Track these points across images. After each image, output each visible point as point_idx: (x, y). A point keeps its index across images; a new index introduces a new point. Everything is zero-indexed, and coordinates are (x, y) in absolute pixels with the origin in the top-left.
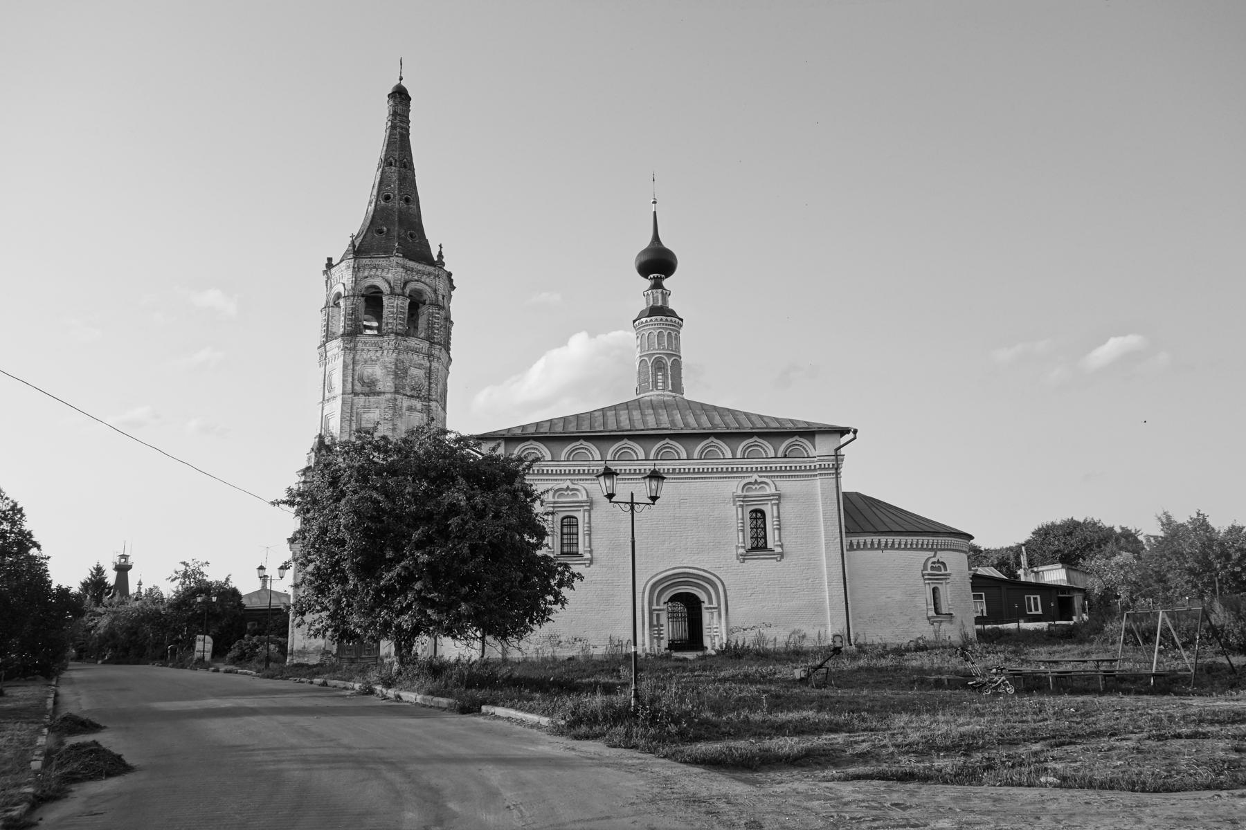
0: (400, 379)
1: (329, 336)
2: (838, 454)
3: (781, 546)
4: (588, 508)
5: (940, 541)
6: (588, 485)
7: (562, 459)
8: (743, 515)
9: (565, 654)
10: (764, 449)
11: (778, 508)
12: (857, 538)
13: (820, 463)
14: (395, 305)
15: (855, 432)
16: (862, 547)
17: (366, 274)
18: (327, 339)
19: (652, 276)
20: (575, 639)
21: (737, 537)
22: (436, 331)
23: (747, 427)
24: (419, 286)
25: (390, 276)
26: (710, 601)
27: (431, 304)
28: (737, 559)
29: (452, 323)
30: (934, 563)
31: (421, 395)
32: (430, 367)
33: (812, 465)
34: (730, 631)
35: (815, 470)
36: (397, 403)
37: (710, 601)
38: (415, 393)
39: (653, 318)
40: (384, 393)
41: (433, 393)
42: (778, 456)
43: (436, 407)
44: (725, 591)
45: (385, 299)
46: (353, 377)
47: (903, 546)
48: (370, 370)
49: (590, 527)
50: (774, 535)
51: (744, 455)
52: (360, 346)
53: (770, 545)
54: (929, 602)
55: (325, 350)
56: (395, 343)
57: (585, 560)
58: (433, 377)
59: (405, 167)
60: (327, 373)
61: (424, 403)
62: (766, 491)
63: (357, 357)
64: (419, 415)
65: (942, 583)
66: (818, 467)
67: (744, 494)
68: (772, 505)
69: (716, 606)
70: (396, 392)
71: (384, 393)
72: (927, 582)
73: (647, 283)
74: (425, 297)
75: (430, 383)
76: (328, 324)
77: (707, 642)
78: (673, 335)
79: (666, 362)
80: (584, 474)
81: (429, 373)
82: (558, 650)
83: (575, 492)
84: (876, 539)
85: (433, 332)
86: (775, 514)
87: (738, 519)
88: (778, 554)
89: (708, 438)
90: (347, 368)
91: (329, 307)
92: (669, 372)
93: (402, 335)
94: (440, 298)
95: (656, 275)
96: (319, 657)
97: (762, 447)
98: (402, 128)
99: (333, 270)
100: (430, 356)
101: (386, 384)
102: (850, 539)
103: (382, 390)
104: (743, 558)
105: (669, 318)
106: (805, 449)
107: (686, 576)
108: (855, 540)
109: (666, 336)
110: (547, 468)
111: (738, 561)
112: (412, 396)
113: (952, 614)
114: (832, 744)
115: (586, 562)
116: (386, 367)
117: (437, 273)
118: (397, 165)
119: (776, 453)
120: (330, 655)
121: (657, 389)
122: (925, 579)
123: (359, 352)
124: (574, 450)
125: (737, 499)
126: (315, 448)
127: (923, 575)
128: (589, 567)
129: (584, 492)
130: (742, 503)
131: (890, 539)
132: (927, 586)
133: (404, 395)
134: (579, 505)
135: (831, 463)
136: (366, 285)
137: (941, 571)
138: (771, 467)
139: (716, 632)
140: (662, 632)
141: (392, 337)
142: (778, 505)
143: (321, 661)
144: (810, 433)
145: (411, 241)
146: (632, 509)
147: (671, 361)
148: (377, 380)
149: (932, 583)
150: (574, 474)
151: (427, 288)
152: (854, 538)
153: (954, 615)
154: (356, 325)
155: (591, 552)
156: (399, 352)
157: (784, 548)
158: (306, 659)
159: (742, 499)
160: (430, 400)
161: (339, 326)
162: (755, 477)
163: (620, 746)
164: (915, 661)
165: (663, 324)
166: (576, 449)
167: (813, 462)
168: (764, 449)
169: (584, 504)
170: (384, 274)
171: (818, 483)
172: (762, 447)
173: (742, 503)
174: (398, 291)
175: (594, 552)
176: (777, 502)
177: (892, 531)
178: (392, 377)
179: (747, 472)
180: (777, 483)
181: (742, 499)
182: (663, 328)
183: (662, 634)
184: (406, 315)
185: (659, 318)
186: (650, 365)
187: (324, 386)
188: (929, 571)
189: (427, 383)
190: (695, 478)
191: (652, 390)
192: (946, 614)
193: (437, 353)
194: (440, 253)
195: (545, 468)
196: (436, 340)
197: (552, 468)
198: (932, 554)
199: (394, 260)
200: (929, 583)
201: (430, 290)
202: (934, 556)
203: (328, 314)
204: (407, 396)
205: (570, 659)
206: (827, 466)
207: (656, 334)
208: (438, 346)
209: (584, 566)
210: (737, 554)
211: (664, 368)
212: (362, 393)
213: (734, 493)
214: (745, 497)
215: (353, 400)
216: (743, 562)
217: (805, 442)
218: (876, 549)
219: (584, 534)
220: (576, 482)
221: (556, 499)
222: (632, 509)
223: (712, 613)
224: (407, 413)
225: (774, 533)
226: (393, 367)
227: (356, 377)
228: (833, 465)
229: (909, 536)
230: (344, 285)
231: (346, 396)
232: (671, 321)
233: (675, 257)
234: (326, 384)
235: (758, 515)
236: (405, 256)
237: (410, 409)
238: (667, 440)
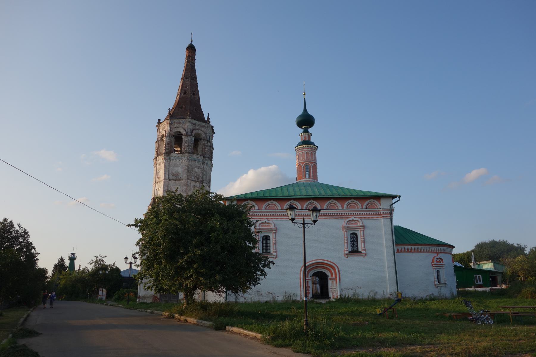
0: (190, 173)
1: (158, 154)
2: (392, 207)
3: (365, 250)
4: (275, 232)
5: (438, 249)
6: (275, 221)
7: (263, 209)
8: (347, 235)
9: (264, 300)
10: (356, 205)
11: (363, 232)
12: (401, 247)
13: (383, 211)
14: (188, 140)
15: (400, 197)
16: (403, 251)
17: (175, 126)
18: (157, 155)
19: (303, 127)
20: (269, 293)
21: (345, 246)
22: (206, 152)
23: (348, 195)
24: (199, 131)
25: (186, 127)
26: (332, 276)
27: (204, 140)
28: (345, 256)
29: (213, 148)
30: (437, 259)
31: (199, 181)
32: (203, 168)
33: (379, 212)
34: (341, 290)
35: (381, 215)
36: (188, 184)
37: (332, 276)
39: (304, 146)
40: (182, 179)
41: (204, 179)
42: (364, 208)
44: (339, 271)
45: (183, 137)
46: (169, 172)
47: (422, 251)
48: (176, 169)
49: (276, 240)
50: (362, 245)
51: (347, 207)
52: (172, 158)
53: (360, 250)
54: (435, 277)
55: (157, 160)
56: (188, 157)
57: (274, 255)
58: (205, 173)
59: (193, 79)
60: (157, 171)
61: (200, 184)
62: (358, 224)
63: (171, 163)
65: (441, 268)
66: (382, 213)
67: (347, 226)
68: (361, 231)
69: (335, 278)
70: (188, 179)
71: (182, 179)
72: (434, 268)
73: (301, 130)
74: (201, 137)
75: (203, 175)
76: (158, 149)
77: (331, 295)
78: (313, 153)
79: (310, 166)
80: (273, 216)
82: (261, 298)
83: (269, 224)
84: (410, 247)
85: (205, 152)
86: (362, 235)
87: (344, 238)
88: (364, 254)
89: (330, 200)
90: (166, 168)
91: (158, 141)
92: (312, 170)
93: (191, 154)
94: (208, 137)
95: (305, 127)
96: (151, 300)
97: (355, 204)
98: (192, 62)
99: (161, 125)
100: (203, 163)
101: (183, 175)
102: (397, 247)
103: (182, 178)
104: (347, 255)
105: (311, 146)
106: (376, 205)
107: (320, 264)
108: (400, 248)
109: (310, 154)
110: (256, 213)
111: (345, 257)
112: (195, 181)
113: (446, 283)
114: (414, 352)
115: (274, 257)
116: (183, 168)
117: (207, 126)
118: (190, 78)
119: (362, 206)
120: (157, 299)
121: (306, 178)
122: (433, 267)
123: (171, 161)
124: (268, 205)
125: (344, 228)
126: (151, 204)
127: (432, 265)
128: (275, 259)
129: (273, 224)
130: (346, 230)
131: (416, 247)
132: (434, 270)
133: (192, 180)
134: (271, 230)
135: (388, 212)
136: (175, 131)
137: (440, 263)
138: (360, 213)
139: (335, 290)
140: (309, 290)
141: (187, 154)
142: (363, 231)
143: (152, 301)
144: (378, 197)
145: (195, 112)
146: (304, 226)
147: (313, 165)
148: (179, 173)
149: (437, 268)
150: (269, 216)
151: (202, 132)
152: (402, 247)
153: (447, 283)
154: (170, 149)
155: (276, 252)
156: (189, 161)
157: (367, 251)
158: (146, 300)
159: (346, 228)
160: (203, 183)
161: (163, 150)
162: (352, 218)
163: (300, 352)
164: (434, 306)
165: (309, 148)
166: (269, 205)
167: (380, 211)
168: (356, 205)
169: (273, 230)
170: (183, 126)
171: (382, 220)
172: (355, 204)
173: (346, 230)
174: (189, 133)
175: (278, 252)
176: (363, 229)
177: (417, 244)
178: (186, 172)
179: (348, 215)
180: (363, 221)
181: (346, 228)
182: (309, 150)
183: (309, 291)
184: (193, 144)
185: (307, 146)
186: (303, 167)
187: (156, 176)
188: (435, 263)
189: (202, 175)
190: (324, 218)
191: (304, 178)
192: (443, 283)
193: (206, 161)
194: (208, 117)
195: (255, 213)
196: (206, 156)
197: (258, 213)
198: (436, 254)
199: (188, 120)
200: (435, 269)
201: (203, 133)
202: (437, 256)
203: (158, 144)
205: (267, 302)
206: (386, 213)
207: (305, 153)
208: (207, 159)
209: (273, 259)
210: (344, 254)
211: (309, 168)
212: (173, 180)
213: (342, 225)
214: (348, 227)
215: (168, 182)
216: (347, 257)
217: (376, 202)
218: (410, 252)
219: (273, 244)
220: (269, 220)
221: (260, 228)
222: (304, 226)
223: (333, 281)
225: (362, 244)
226: (187, 167)
227: (170, 172)
228: (389, 212)
229: (425, 246)
230: (165, 131)
231: (166, 181)
232: (312, 147)
233: (314, 118)
234: (157, 176)
235: (354, 236)
236: (193, 118)
238: (311, 201)
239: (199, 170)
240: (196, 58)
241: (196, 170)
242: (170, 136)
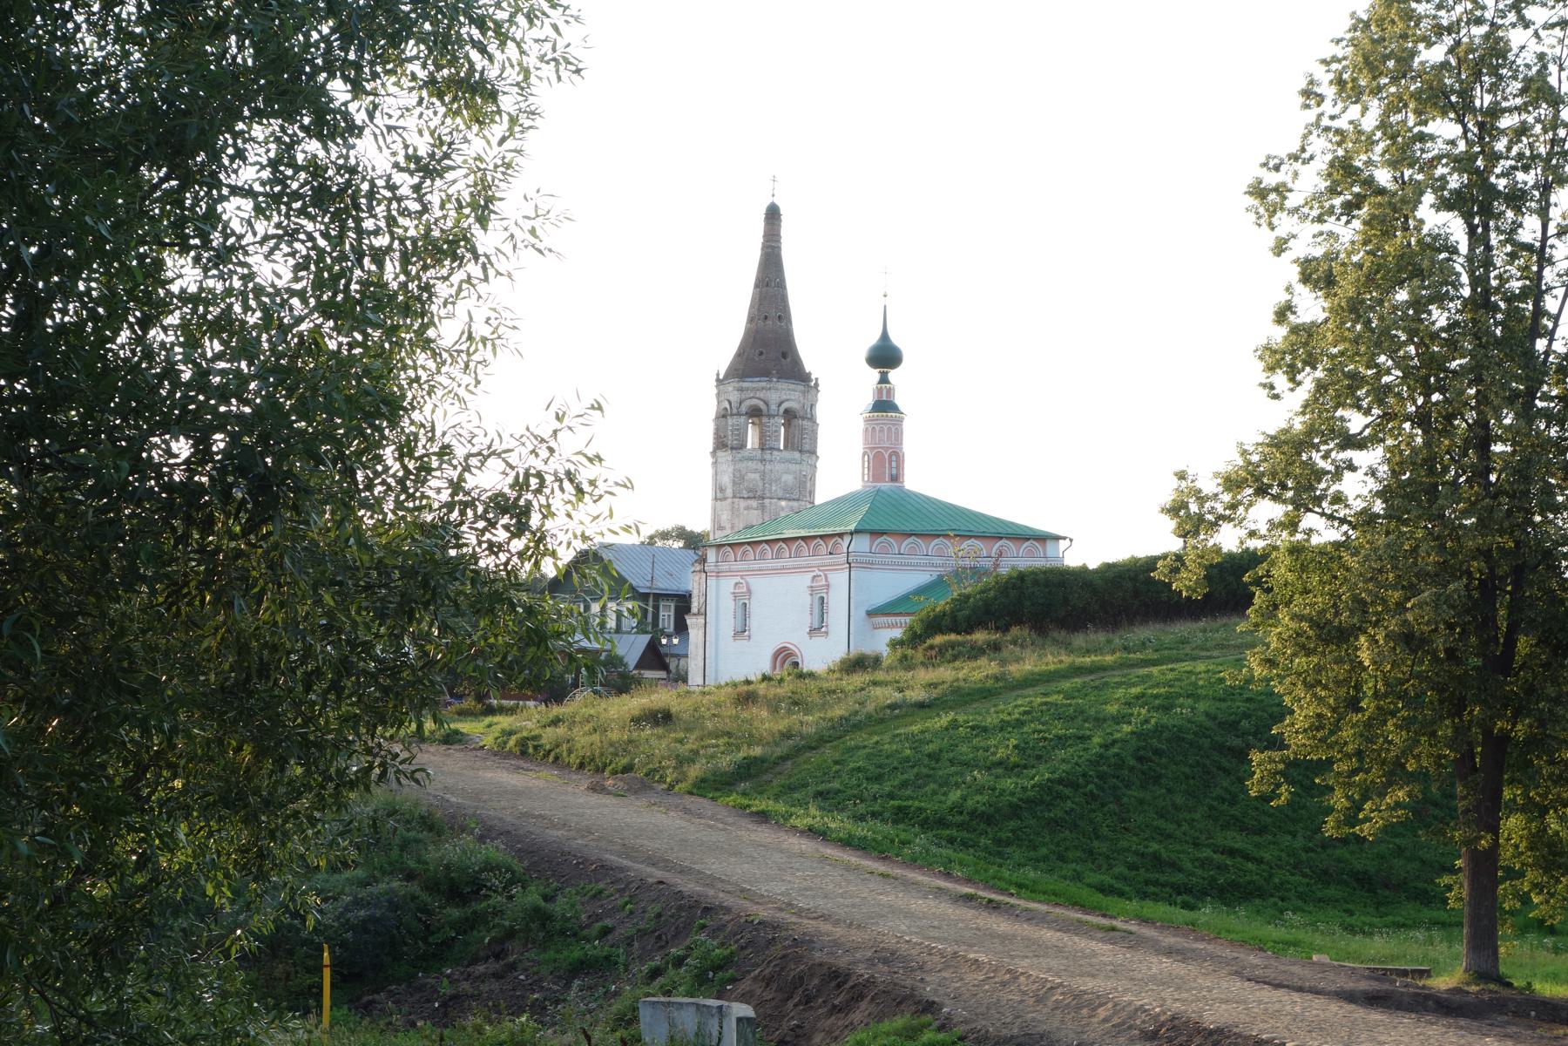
24: (755, 402)
38: (751, 495)
70: (734, 497)
100: (763, 460)
101: (729, 492)
237: (747, 508)
239: (757, 476)
241: (752, 476)
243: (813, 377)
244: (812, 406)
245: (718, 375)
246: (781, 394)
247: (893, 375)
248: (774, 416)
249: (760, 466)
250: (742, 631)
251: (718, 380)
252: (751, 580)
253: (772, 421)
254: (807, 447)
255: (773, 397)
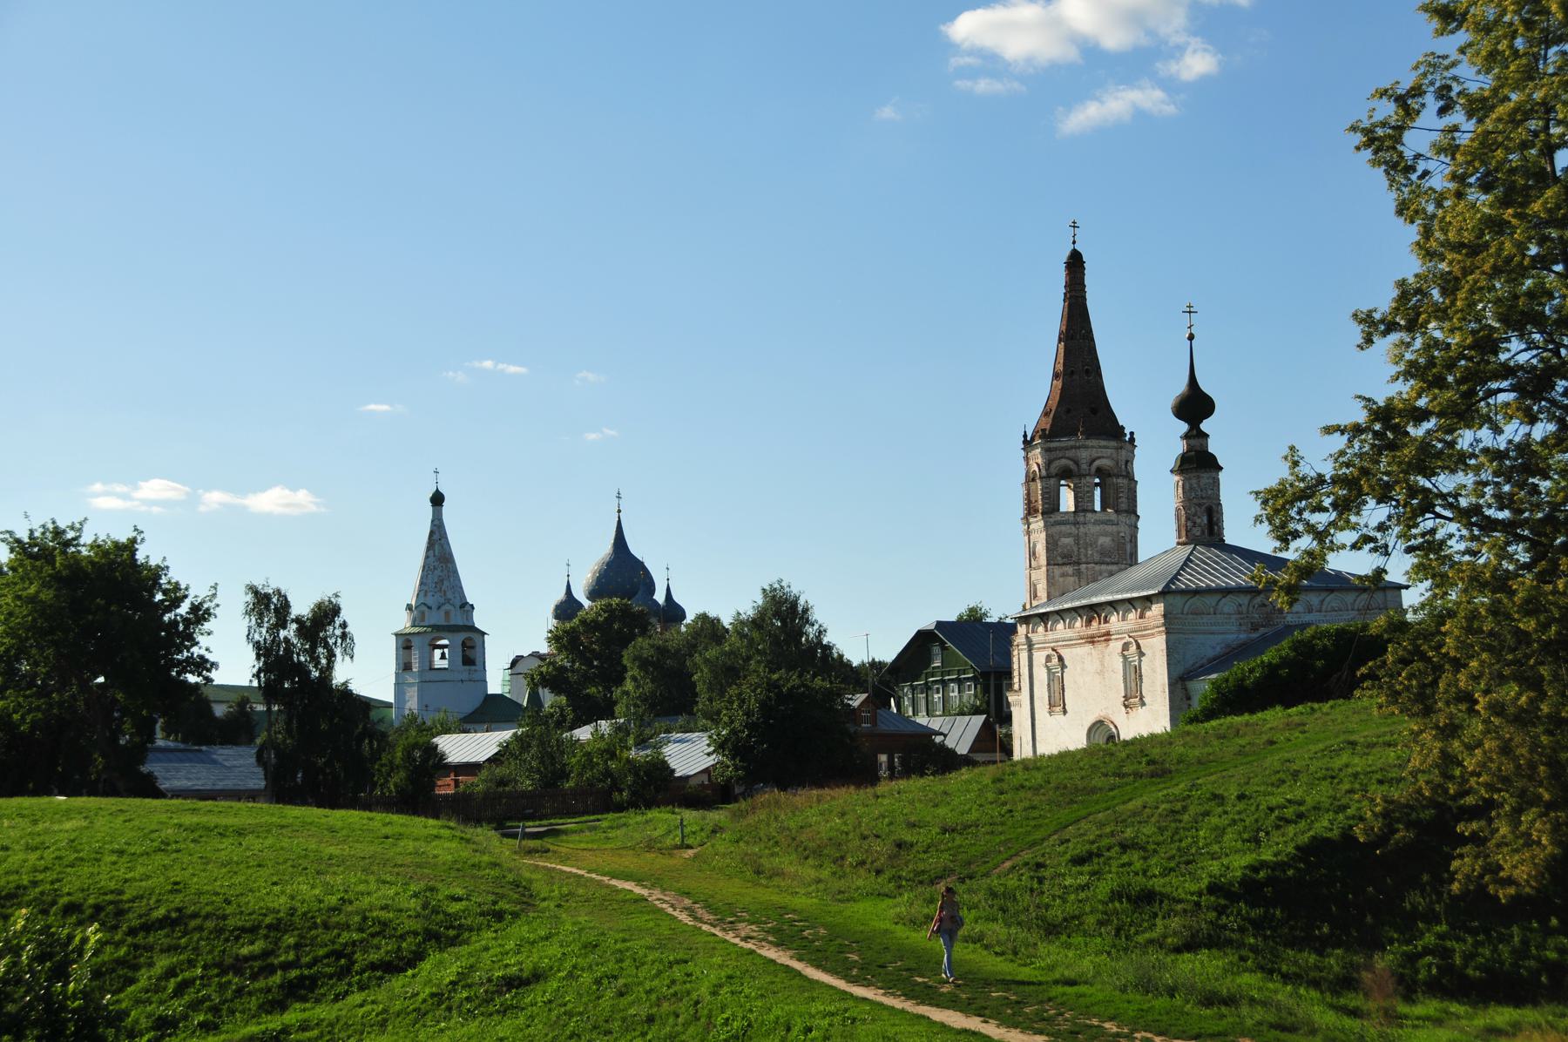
24: (1064, 462)
41: (1082, 557)
43: (1087, 568)
64: (1072, 579)
81: (1077, 538)
112: (1064, 564)
160: (1079, 564)
204: (1058, 565)
224: (1061, 579)
234: (1032, 554)
237: (1063, 575)
240: (1086, 283)
242: (1049, 476)
243: (1127, 431)
244: (1127, 462)
245: (1025, 436)
246: (1097, 451)
247: (1205, 426)
248: (1085, 476)
249: (1073, 530)
250: (1058, 702)
251: (1026, 442)
252: (1063, 652)
253: (1083, 481)
254: (1124, 506)
255: (1084, 455)
